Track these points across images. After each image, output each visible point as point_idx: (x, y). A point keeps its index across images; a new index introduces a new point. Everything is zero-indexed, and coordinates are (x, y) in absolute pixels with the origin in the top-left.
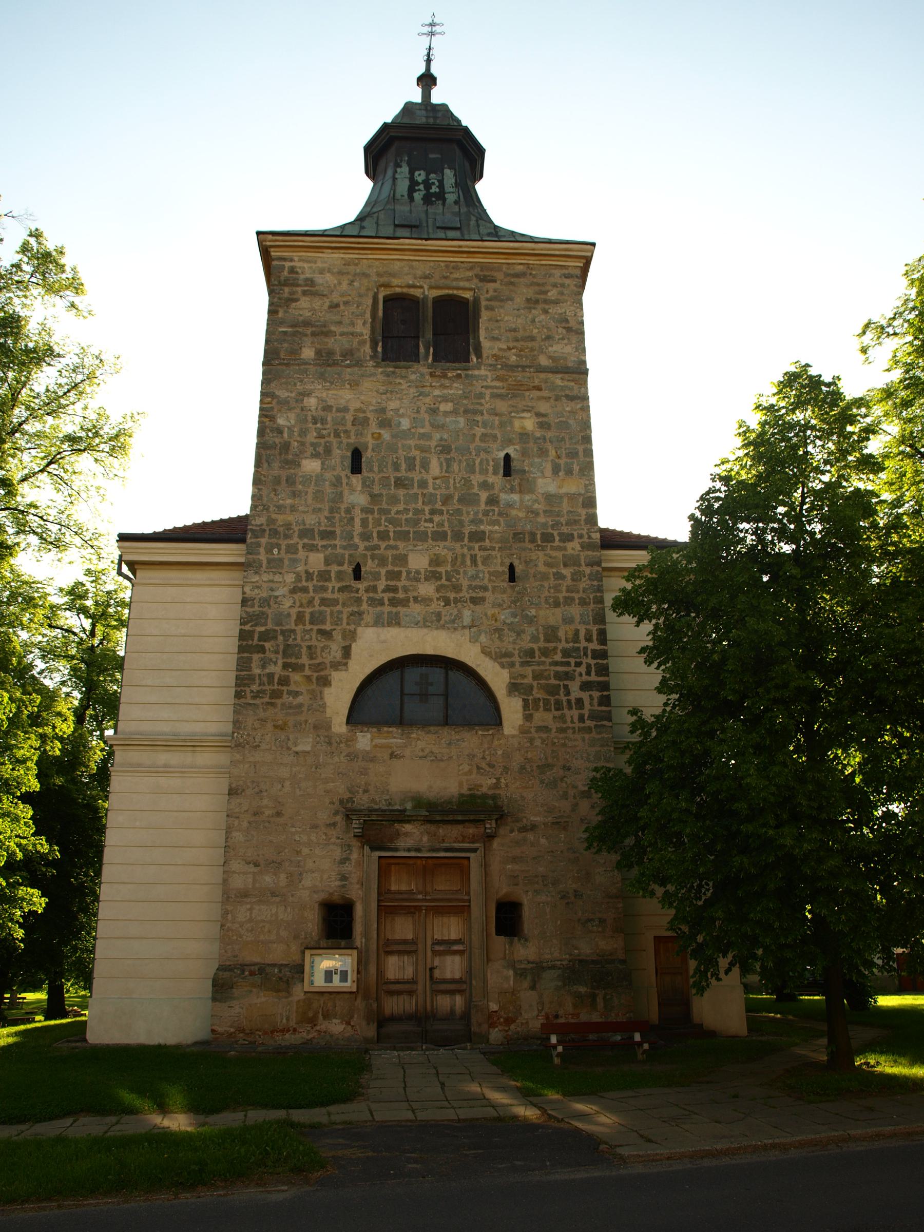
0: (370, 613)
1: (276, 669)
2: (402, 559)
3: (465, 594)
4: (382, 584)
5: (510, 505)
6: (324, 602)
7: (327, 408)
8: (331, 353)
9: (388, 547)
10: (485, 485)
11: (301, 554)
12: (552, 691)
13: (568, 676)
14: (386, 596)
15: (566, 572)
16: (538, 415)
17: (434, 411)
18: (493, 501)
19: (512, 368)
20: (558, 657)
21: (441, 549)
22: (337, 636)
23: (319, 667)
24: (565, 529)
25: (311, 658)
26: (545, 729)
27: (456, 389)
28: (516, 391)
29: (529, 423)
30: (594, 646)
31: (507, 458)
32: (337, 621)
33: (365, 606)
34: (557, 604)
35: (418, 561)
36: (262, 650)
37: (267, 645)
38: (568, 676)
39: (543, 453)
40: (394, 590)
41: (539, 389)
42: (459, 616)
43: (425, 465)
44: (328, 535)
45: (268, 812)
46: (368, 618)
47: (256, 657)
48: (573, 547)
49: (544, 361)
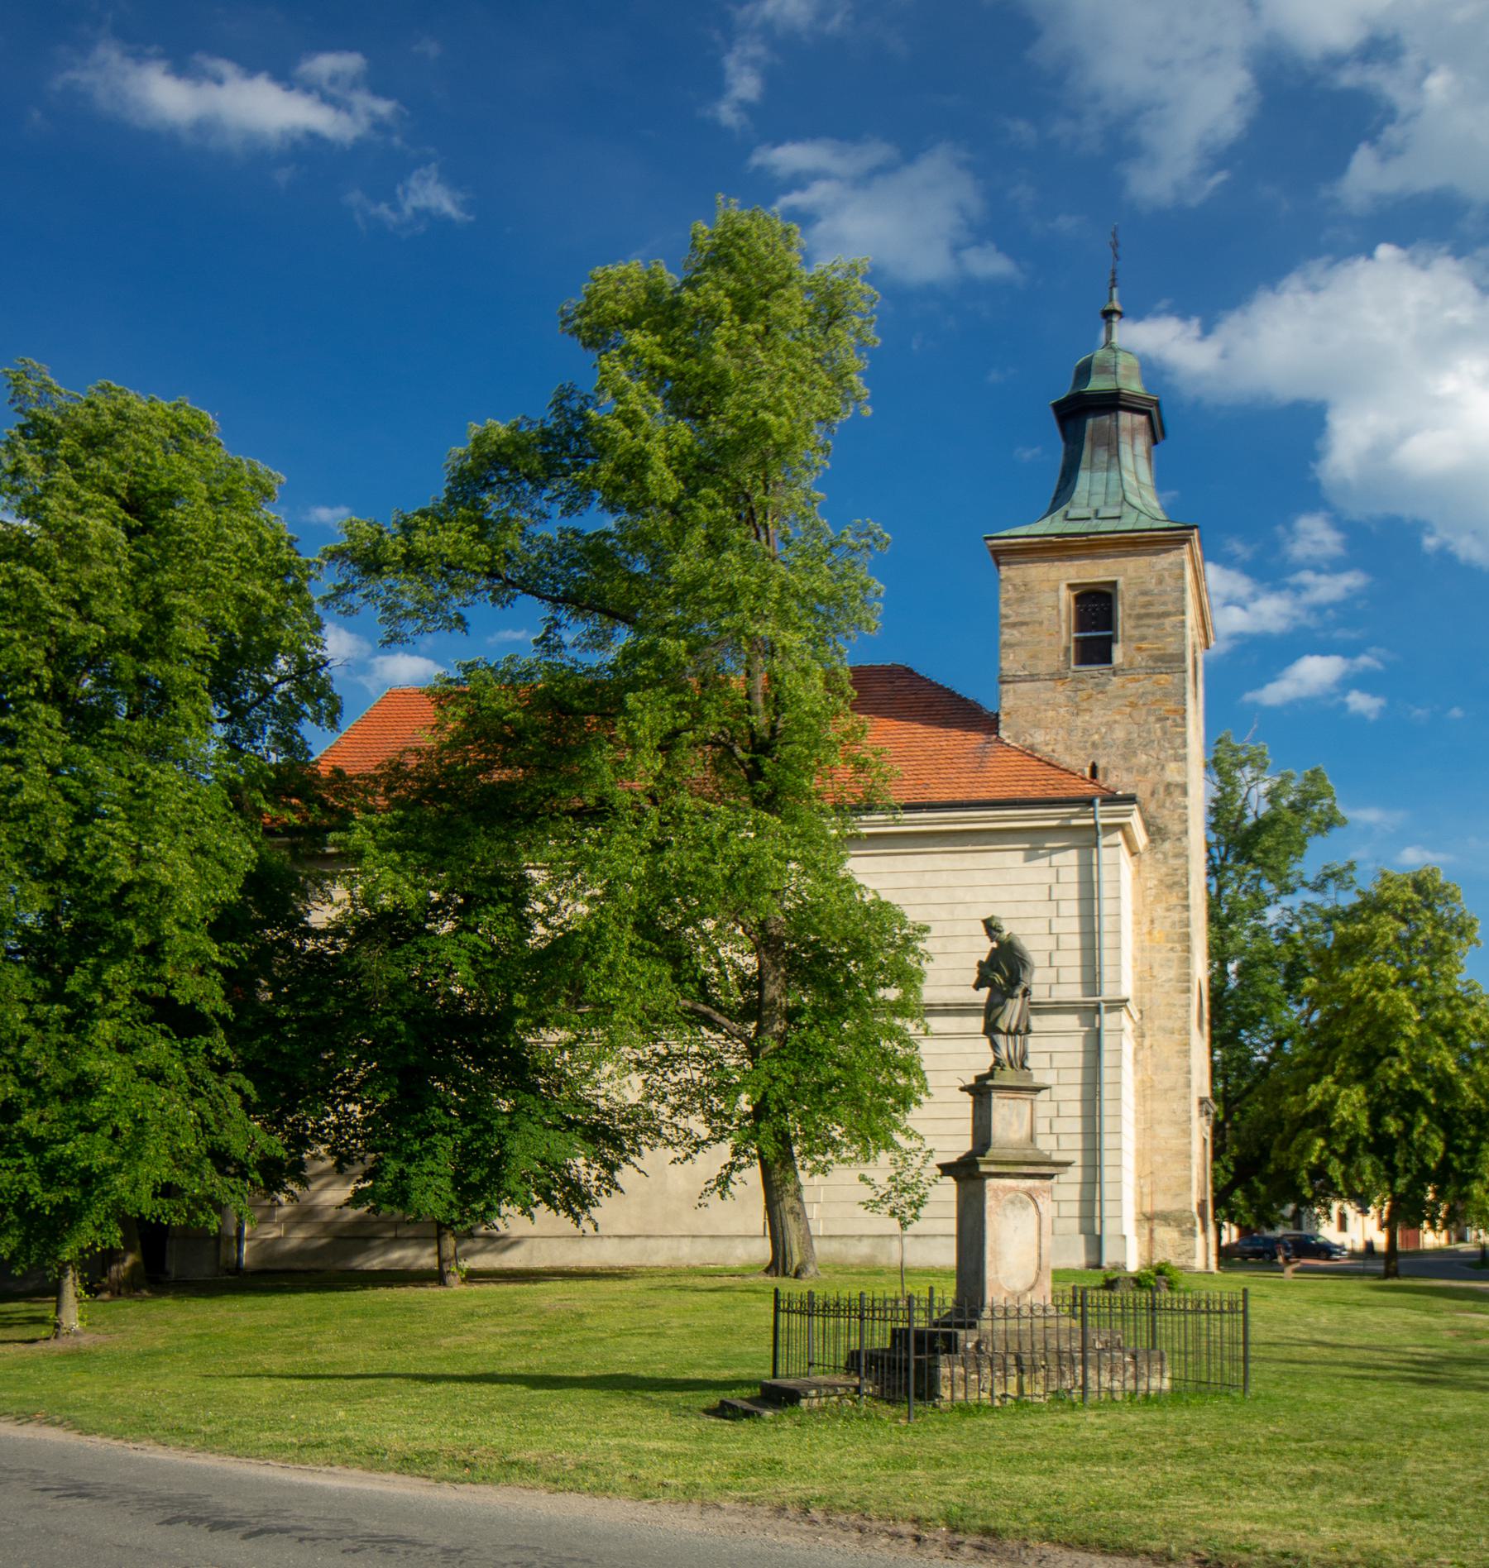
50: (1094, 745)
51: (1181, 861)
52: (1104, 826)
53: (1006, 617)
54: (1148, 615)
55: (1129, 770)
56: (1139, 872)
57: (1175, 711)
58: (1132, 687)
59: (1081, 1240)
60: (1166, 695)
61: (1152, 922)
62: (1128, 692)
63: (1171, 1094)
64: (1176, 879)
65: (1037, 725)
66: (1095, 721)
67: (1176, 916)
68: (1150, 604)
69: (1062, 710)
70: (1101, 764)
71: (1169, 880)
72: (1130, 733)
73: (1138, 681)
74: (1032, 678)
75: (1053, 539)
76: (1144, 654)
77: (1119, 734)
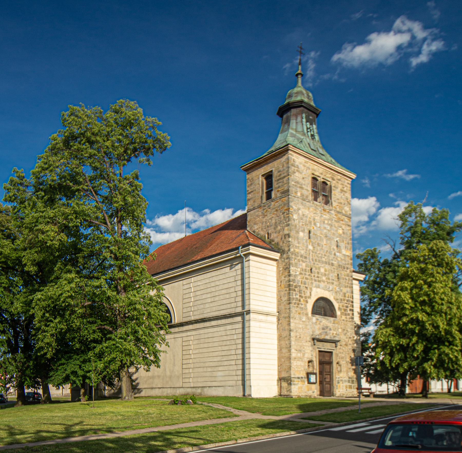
0: (315, 283)
1: (298, 297)
2: (319, 268)
3: (331, 281)
4: (316, 275)
5: (338, 256)
6: (306, 279)
7: (303, 215)
8: (303, 196)
9: (318, 264)
10: (334, 249)
11: (301, 263)
12: (345, 310)
13: (347, 307)
14: (317, 279)
15: (347, 278)
16: (343, 229)
17: (324, 222)
18: (335, 254)
19: (338, 212)
20: (346, 302)
21: (327, 267)
22: (309, 289)
23: (306, 297)
24: (347, 266)
25: (305, 294)
26: (343, 320)
27: (327, 216)
28: (339, 220)
29: (340, 231)
30: (351, 299)
31: (337, 241)
32: (308, 285)
33: (313, 281)
34: (345, 287)
35: (322, 270)
36: (295, 291)
37: (296, 289)
38: (347, 307)
39: (343, 241)
40: (318, 277)
41: (342, 220)
42: (329, 288)
43: (323, 240)
44: (306, 258)
45: (298, 337)
46: (314, 285)
47: (294, 292)
48: (348, 271)
49: (344, 212)
50: (268, 227)
51: (288, 260)
52: (244, 255)
53: (248, 191)
54: (280, 179)
55: (276, 233)
56: (278, 266)
57: (286, 210)
58: (277, 204)
59: (241, 387)
60: (285, 205)
61: (281, 282)
62: (276, 206)
63: (286, 338)
64: (287, 266)
65: (255, 224)
66: (268, 219)
67: (287, 279)
68: (281, 175)
69: (260, 217)
70: (270, 232)
71: (285, 267)
72: (276, 220)
73: (277, 202)
74: (254, 209)
75: (256, 162)
76: (279, 192)
77: (274, 221)
